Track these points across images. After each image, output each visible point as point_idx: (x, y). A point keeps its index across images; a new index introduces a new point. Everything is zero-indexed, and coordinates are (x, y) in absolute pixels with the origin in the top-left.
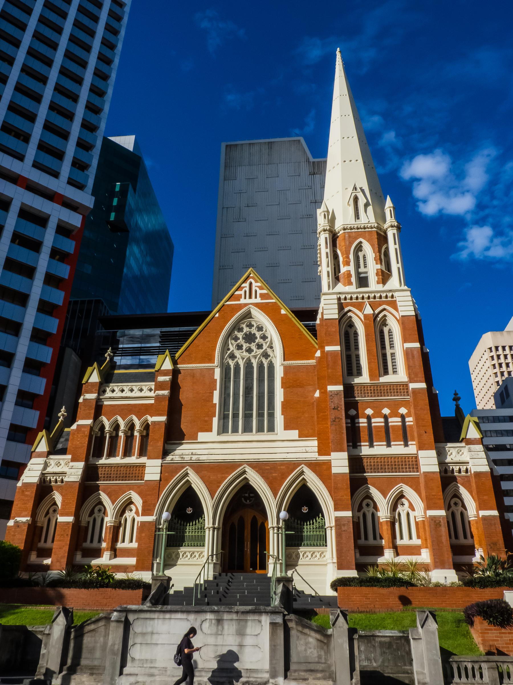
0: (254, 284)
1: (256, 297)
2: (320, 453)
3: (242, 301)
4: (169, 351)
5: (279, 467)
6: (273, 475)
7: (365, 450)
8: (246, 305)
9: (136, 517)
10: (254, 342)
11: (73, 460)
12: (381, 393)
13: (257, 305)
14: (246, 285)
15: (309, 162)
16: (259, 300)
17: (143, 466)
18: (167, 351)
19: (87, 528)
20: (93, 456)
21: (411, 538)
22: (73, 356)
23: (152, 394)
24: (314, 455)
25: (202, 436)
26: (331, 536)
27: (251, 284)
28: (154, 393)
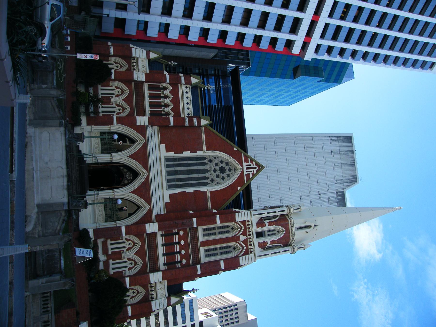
0: (255, 170)
1: (247, 172)
2: (157, 216)
3: (244, 164)
4: (213, 123)
5: (147, 193)
6: (143, 190)
8: (242, 166)
9: (116, 113)
10: (220, 173)
11: (146, 74)
12: (194, 248)
13: (243, 172)
14: (255, 166)
15: (344, 188)
16: (245, 173)
17: (144, 115)
18: (212, 122)
19: (109, 86)
20: (148, 85)
21: (113, 269)
22: (213, 54)
23: (186, 115)
24: (155, 212)
25: (163, 147)
26: (111, 224)
27: (255, 168)
28: (187, 117)
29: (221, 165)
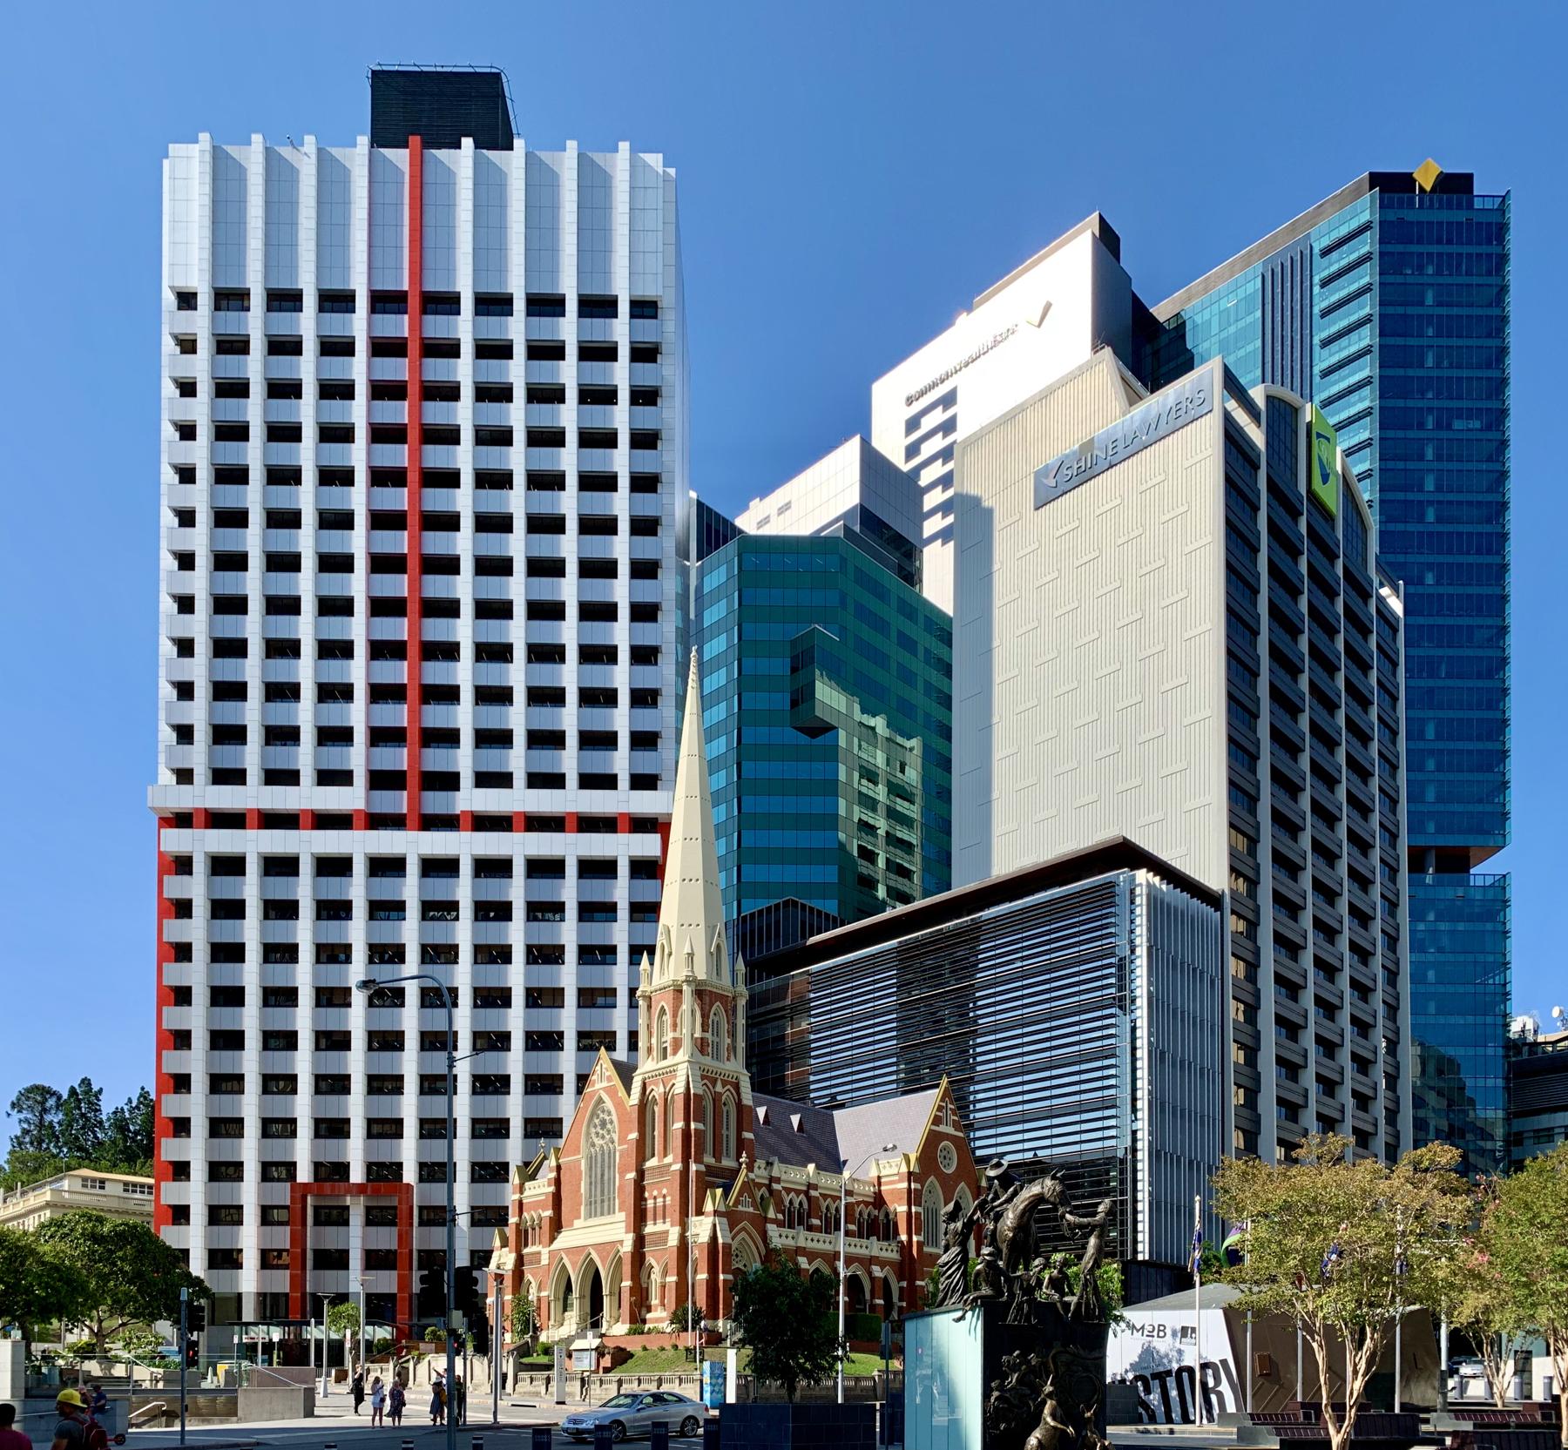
3: (597, 1086)
7: (649, 1228)
13: (604, 1089)
16: (605, 1084)
29: (598, 1129)
